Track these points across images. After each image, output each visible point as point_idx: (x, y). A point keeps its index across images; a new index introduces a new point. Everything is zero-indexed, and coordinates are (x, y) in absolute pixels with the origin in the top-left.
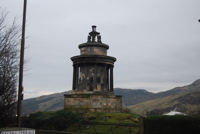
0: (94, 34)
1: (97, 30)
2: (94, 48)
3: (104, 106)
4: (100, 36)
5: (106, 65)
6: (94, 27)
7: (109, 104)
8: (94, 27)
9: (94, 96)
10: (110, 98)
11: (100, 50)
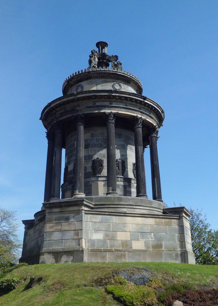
3: (92, 242)
7: (121, 236)
8: (102, 45)
9: (57, 210)
10: (125, 215)
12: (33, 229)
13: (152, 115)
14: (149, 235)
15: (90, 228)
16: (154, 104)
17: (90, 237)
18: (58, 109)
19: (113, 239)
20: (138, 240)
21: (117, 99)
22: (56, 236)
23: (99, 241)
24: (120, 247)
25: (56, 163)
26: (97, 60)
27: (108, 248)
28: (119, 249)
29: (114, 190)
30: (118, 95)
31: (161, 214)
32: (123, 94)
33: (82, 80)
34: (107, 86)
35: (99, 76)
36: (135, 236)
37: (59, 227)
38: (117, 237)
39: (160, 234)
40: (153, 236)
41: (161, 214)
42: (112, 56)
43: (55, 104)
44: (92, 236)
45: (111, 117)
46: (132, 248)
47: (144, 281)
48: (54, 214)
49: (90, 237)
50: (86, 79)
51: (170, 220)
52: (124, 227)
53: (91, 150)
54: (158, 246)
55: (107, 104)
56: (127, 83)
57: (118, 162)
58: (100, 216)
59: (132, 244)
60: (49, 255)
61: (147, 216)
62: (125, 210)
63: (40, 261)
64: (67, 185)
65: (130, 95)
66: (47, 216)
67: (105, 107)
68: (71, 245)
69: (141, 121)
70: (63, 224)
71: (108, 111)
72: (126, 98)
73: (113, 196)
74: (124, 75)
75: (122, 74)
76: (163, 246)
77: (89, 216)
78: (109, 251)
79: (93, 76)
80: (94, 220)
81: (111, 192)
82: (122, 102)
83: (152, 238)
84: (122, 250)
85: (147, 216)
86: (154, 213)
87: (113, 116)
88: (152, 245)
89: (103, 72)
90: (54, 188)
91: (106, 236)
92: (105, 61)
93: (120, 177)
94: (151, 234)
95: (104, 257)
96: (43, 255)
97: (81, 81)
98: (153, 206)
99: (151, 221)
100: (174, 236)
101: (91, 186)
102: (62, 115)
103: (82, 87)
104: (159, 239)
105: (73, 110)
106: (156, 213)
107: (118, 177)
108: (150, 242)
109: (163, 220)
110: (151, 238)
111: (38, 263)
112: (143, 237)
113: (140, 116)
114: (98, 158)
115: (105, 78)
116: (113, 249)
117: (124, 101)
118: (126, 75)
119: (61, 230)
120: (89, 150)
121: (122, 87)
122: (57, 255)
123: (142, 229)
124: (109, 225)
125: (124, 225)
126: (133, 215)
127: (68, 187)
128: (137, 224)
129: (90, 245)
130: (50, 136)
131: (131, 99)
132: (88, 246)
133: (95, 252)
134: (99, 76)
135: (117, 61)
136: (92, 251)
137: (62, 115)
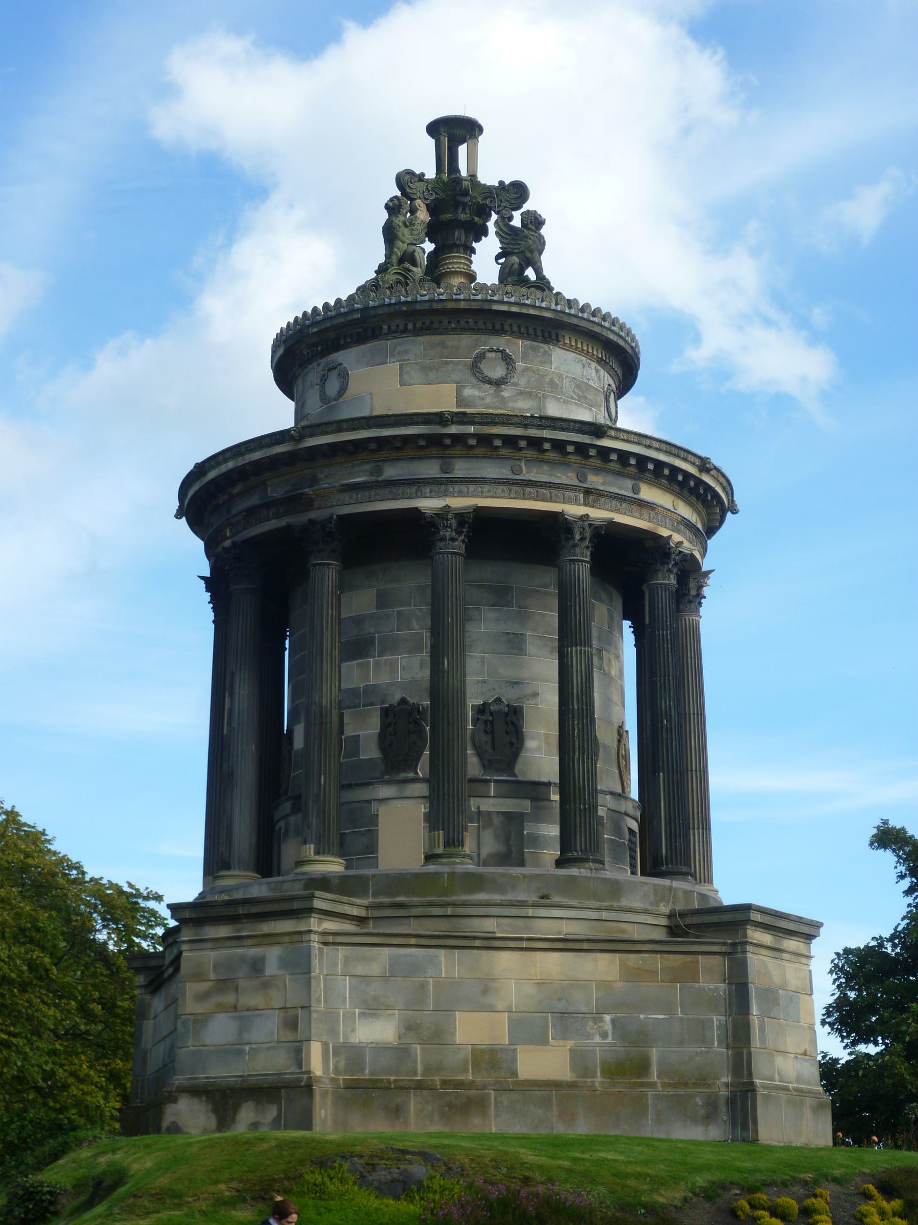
1: (490, 165)
2: (347, 357)
3: (354, 1055)
4: (534, 222)
7: (471, 1030)
8: (453, 132)
9: (223, 931)
10: (491, 943)
11: (425, 369)
13: (648, 493)
14: (591, 1023)
15: (345, 999)
16: (649, 447)
17: (346, 1036)
18: (235, 491)
19: (438, 1036)
20: (544, 1041)
21: (472, 447)
22: (220, 1030)
23: (380, 1048)
24: (465, 1071)
25: (235, 724)
26: (423, 216)
27: (415, 1074)
28: (460, 1077)
29: (454, 842)
30: (471, 429)
32: (495, 424)
33: (342, 342)
34: (450, 367)
35: (410, 326)
36: (529, 1031)
37: (229, 999)
38: (453, 1034)
39: (642, 1016)
40: (608, 1027)
42: (501, 183)
43: (224, 468)
44: (353, 1030)
45: (445, 527)
46: (514, 1074)
47: (402, 1187)
48: (209, 945)
49: (346, 1036)
50: (361, 339)
51: (688, 958)
52: (486, 991)
53: (377, 663)
54: (629, 1068)
55: (430, 469)
56: (545, 341)
57: (491, 714)
58: (386, 951)
59: (514, 1060)
60: (196, 1101)
61: (585, 946)
62: (489, 925)
63: (165, 1124)
64: (288, 811)
65: (526, 426)
67: (419, 484)
68: (270, 1063)
69: (588, 534)
70: (242, 983)
71: (429, 504)
72: (510, 441)
73: (446, 869)
74: (525, 311)
75: (515, 309)
76: (654, 1070)
77: (342, 951)
78: (420, 1086)
79: (385, 327)
80: (360, 970)
81: (440, 850)
82: (498, 457)
83: (604, 1035)
84: (472, 1082)
85: (585, 946)
86: (623, 931)
87: (454, 526)
88: (603, 1063)
89: (427, 306)
91: (410, 1027)
92: (463, 217)
93: (496, 781)
94: (602, 1020)
95: (397, 1112)
96: (175, 1101)
97: (338, 347)
98: (624, 903)
99: (603, 967)
100: (704, 1024)
101: (374, 820)
102: (252, 514)
103: (344, 376)
104: (635, 1038)
105: (295, 502)
106: (635, 933)
107: (490, 781)
108: (594, 1052)
109: (659, 962)
110: (601, 1039)
111: (158, 1130)
112: (564, 1035)
113: (581, 510)
114: (403, 701)
116: (437, 1079)
117: (506, 452)
118: (532, 312)
119: (235, 1008)
120: (368, 664)
121: (520, 365)
122: (224, 1099)
123: (560, 1000)
124: (423, 986)
125: (487, 986)
126: (524, 944)
127: (292, 819)
128: (541, 984)
129: (342, 1065)
131: (535, 443)
132: (336, 1068)
133: (366, 1088)
134: (410, 326)
135: (526, 207)
136: (352, 1086)
137: (252, 514)
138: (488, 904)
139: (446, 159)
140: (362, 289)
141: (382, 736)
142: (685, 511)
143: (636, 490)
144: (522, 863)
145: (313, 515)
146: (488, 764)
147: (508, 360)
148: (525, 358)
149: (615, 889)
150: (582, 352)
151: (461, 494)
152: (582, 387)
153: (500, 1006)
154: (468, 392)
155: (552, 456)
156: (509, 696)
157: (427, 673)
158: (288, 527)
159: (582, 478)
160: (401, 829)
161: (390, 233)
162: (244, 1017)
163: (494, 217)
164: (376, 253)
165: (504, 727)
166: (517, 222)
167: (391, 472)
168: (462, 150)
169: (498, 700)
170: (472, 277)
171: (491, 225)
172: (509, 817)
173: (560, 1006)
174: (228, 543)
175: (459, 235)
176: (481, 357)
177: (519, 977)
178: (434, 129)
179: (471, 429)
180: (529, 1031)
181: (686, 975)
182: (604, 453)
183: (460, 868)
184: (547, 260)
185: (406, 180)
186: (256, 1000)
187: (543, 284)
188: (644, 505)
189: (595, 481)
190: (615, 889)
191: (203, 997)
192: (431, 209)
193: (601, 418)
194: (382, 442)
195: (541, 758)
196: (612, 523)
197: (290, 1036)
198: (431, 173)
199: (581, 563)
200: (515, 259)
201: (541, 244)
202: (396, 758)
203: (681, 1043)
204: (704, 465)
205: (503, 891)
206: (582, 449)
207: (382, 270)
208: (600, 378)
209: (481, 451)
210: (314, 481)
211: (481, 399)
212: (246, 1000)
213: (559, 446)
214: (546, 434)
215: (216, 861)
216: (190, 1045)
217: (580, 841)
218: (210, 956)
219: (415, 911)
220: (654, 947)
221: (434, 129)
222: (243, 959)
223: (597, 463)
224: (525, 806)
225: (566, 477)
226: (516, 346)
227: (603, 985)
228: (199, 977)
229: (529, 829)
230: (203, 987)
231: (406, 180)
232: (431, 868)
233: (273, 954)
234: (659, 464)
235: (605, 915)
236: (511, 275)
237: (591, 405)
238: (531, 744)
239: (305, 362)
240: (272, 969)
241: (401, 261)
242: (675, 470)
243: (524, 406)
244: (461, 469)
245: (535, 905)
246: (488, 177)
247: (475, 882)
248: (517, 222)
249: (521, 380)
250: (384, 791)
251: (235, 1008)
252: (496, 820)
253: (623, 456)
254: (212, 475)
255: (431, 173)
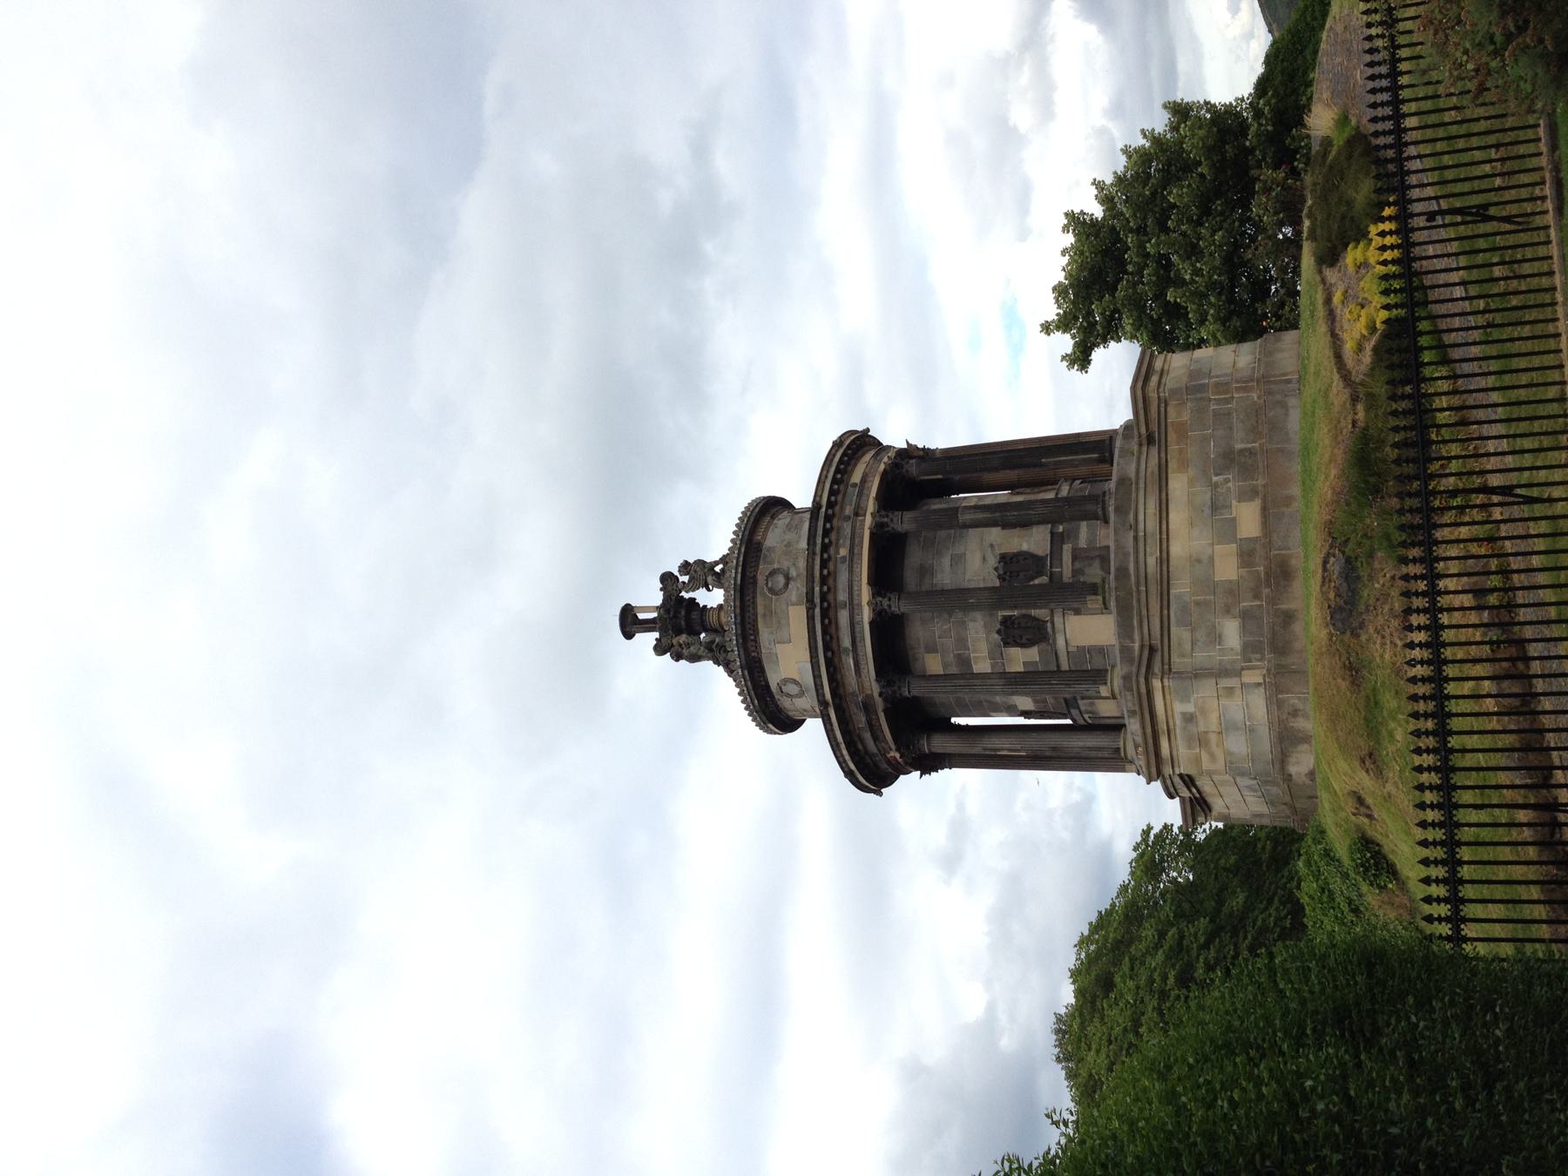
0: (678, 626)
1: (650, 597)
2: (773, 680)
3: (1250, 649)
4: (686, 567)
5: (886, 602)
6: (630, 622)
7: (1228, 569)
8: (630, 622)
10: (1164, 560)
12: (1210, 800)
13: (856, 477)
19: (1232, 590)
20: (1234, 519)
23: (1244, 629)
26: (683, 638)
29: (1093, 589)
30: (817, 589)
31: (1154, 451)
36: (1227, 530)
37: (1213, 738)
41: (1154, 451)
43: (847, 757)
46: (1255, 540)
50: (762, 670)
52: (1199, 561)
55: (843, 617)
58: (1173, 629)
62: (1152, 561)
66: (1183, 769)
70: (1202, 728)
71: (866, 615)
72: (824, 564)
77: (1175, 659)
80: (1188, 647)
90: (1090, 749)
91: (1227, 611)
97: (768, 686)
98: (1133, 475)
99: (1178, 485)
100: (1216, 414)
101: (1081, 649)
103: (786, 681)
104: (1229, 459)
109: (1173, 448)
110: (1231, 483)
114: (999, 632)
115: (756, 620)
121: (776, 566)
124: (1197, 604)
130: (929, 764)
131: (825, 548)
138: (1137, 562)
139: (647, 626)
140: (730, 672)
141: (1022, 646)
142: (868, 457)
143: (855, 485)
144: (1108, 547)
145: (876, 694)
146: (1040, 574)
147: (773, 573)
148: (772, 563)
149: (1123, 481)
150: (767, 529)
151: (860, 595)
152: (789, 527)
153: (1209, 551)
154: (794, 598)
155: (833, 536)
156: (992, 561)
157: (978, 615)
158: (885, 711)
159: (847, 518)
160: (1088, 630)
161: (694, 658)
162: (1227, 727)
163: (683, 594)
164: (708, 666)
165: (1012, 565)
166: (685, 579)
167: (846, 642)
168: (641, 616)
169: (996, 569)
170: (720, 607)
171: (686, 595)
172: (1075, 558)
173: (1208, 511)
174: (898, 755)
175: (695, 615)
176: (771, 590)
177: (1187, 538)
178: (628, 635)
179: (817, 589)
180: (1227, 530)
181: (1182, 430)
182: (830, 505)
183: (1113, 585)
184: (710, 558)
185: (660, 649)
186: (1214, 717)
187: (724, 560)
188: (864, 480)
189: (848, 511)
190: (1123, 481)
191: (1212, 756)
192: (678, 632)
193: (808, 515)
194: (827, 647)
195: (1035, 541)
196: (877, 498)
197: (1238, 692)
198: (656, 635)
199: (903, 522)
200: (710, 579)
201: (700, 563)
202: (1036, 634)
203: (1231, 428)
204: (837, 445)
205: (1126, 555)
206: (828, 519)
207: (717, 663)
208: (784, 519)
209: (831, 581)
210: (853, 694)
211: (797, 590)
212: (1214, 727)
213: (826, 533)
214: (819, 541)
215: (1113, 761)
216: (1247, 765)
217: (1090, 507)
218: (1182, 751)
219: (1144, 612)
220: (1164, 448)
221: (628, 635)
222: (1184, 729)
223: (837, 508)
224: (1067, 549)
225: (847, 528)
226: (763, 569)
227: (1191, 483)
228: (1198, 760)
229: (1083, 543)
230: (1205, 757)
231: (660, 649)
232: (1113, 604)
233: (1179, 708)
234: (837, 471)
235: (1142, 485)
236: (719, 579)
237: (802, 521)
238: (1025, 547)
239: (779, 710)
240: (1190, 708)
241: (711, 650)
242: (841, 461)
243: (802, 564)
244: (842, 596)
245: (1136, 531)
246: (657, 598)
247: (1122, 572)
248: (685, 579)
249: (786, 564)
250: (1061, 642)
251: (1220, 733)
252: (1078, 565)
253: (832, 492)
254: (852, 767)
255: (656, 635)
